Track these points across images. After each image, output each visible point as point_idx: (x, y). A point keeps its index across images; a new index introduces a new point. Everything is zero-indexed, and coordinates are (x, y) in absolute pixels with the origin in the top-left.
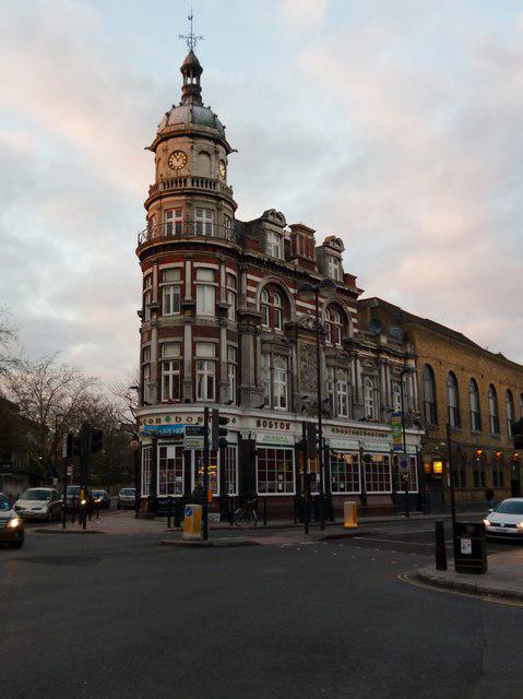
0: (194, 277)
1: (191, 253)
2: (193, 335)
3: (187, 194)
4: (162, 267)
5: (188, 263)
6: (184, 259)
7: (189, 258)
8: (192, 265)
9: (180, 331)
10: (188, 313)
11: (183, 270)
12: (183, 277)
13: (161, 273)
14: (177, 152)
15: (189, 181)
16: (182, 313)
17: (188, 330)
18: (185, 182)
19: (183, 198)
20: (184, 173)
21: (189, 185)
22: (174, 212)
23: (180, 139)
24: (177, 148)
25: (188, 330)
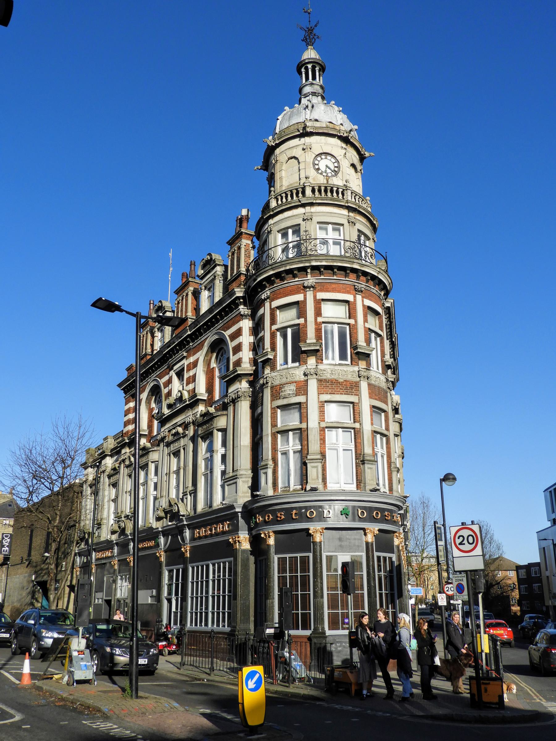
4: (276, 303)
8: (315, 297)
10: (362, 364)
12: (352, 314)
13: (273, 312)
17: (364, 386)
18: (304, 193)
19: (345, 212)
20: (337, 181)
22: (290, 231)
25: (364, 386)
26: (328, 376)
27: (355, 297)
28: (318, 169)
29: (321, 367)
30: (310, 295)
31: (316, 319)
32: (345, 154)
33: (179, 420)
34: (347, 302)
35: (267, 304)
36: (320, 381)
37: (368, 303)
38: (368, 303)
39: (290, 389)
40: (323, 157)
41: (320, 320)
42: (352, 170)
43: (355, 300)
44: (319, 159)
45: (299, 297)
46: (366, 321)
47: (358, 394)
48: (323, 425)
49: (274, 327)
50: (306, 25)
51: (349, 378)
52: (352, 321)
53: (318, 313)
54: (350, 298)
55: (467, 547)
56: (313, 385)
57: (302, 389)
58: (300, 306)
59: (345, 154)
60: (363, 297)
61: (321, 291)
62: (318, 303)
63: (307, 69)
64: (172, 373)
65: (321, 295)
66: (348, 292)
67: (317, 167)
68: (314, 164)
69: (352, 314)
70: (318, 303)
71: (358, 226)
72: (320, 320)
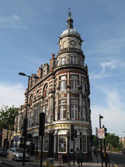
0: (70, 78)
1: (81, 71)
3: (78, 53)
5: (68, 73)
7: (80, 73)
8: (69, 74)
10: (80, 90)
11: (78, 76)
12: (78, 78)
14: (73, 41)
16: (66, 89)
17: (80, 95)
19: (77, 54)
21: (78, 50)
23: (74, 37)
24: (73, 40)
25: (80, 95)
31: (69, 79)
33: (37, 102)
34: (77, 75)
35: (58, 75)
37: (82, 75)
38: (82, 75)
39: (63, 96)
41: (70, 79)
45: (66, 74)
46: (81, 80)
47: (79, 97)
49: (60, 81)
50: (69, 12)
51: (77, 93)
52: (78, 80)
54: (78, 74)
55: (101, 133)
56: (68, 95)
58: (66, 76)
63: (69, 21)
64: (36, 91)
65: (71, 73)
66: (77, 73)
69: (78, 78)
71: (80, 57)
72: (70, 79)
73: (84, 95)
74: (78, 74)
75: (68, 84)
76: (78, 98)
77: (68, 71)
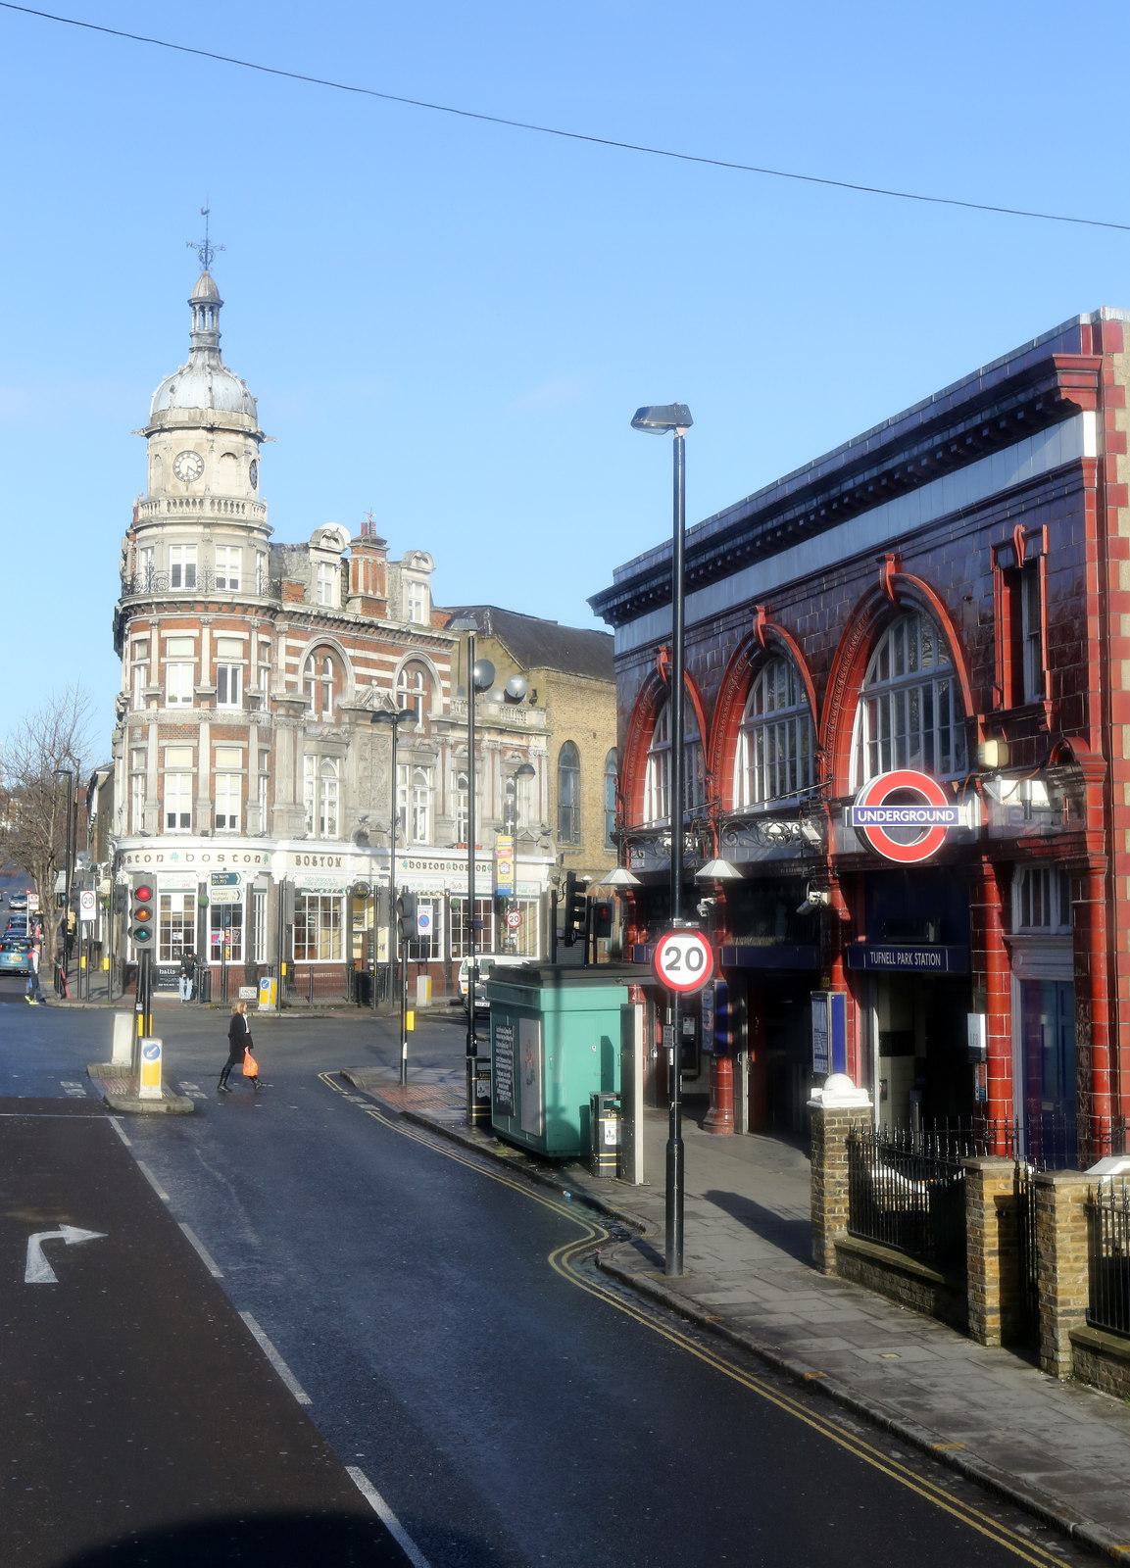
0: (162, 652)
1: (211, 616)
2: (213, 737)
6: (146, 626)
9: (193, 731)
10: (205, 705)
12: (198, 652)
15: (207, 503)
16: (148, 706)
17: (205, 729)
19: (200, 529)
20: (198, 487)
25: (205, 729)
26: (168, 721)
27: (201, 631)
28: (179, 473)
29: (162, 711)
30: (155, 632)
32: (212, 447)
36: (160, 726)
40: (185, 456)
42: (229, 460)
43: (201, 634)
44: (180, 459)
48: (161, 770)
52: (196, 660)
53: (162, 652)
56: (153, 731)
57: (145, 736)
59: (212, 447)
60: (211, 629)
61: (165, 628)
62: (163, 642)
66: (194, 627)
67: (177, 470)
68: (175, 467)
69: (198, 652)
70: (163, 642)
72: (163, 660)
73: (225, 722)
74: (195, 633)
75: (154, 683)
76: (194, 742)
77: (152, 624)
